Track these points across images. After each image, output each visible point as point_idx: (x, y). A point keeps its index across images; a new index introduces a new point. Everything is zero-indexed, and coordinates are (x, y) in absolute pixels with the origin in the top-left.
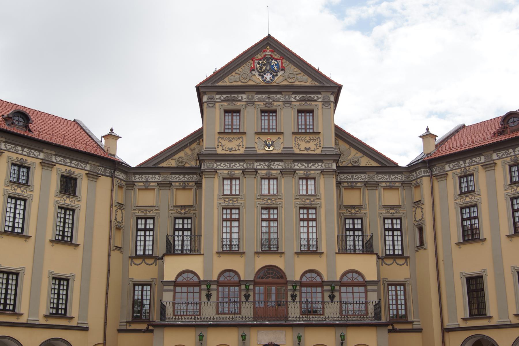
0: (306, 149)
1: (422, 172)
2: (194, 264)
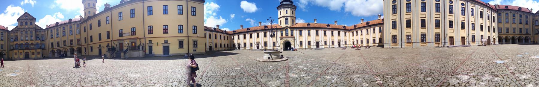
2: (17, 42)
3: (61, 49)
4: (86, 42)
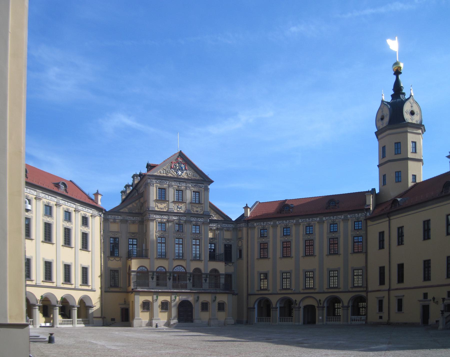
0: (197, 211)
1: (243, 225)
4: (382, 282)
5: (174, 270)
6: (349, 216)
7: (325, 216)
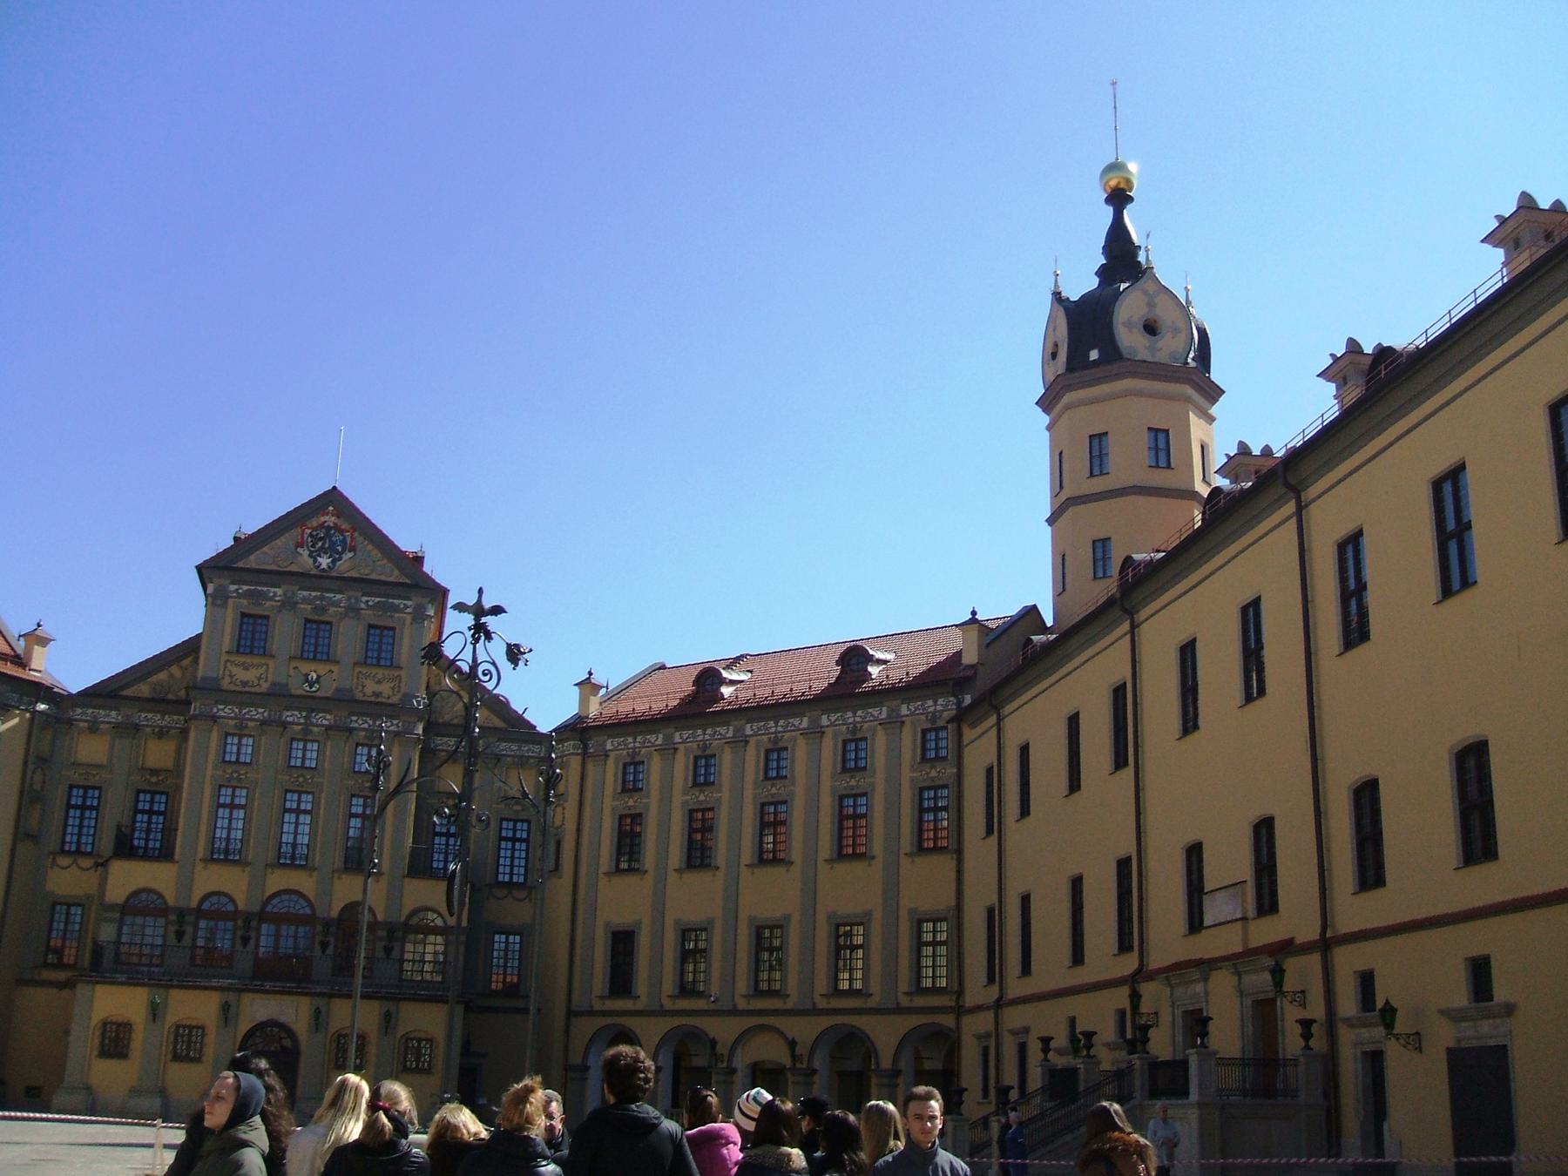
2: (158, 877)
3: (723, 1030)
5: (269, 909)
6: (904, 710)
7: (827, 712)
